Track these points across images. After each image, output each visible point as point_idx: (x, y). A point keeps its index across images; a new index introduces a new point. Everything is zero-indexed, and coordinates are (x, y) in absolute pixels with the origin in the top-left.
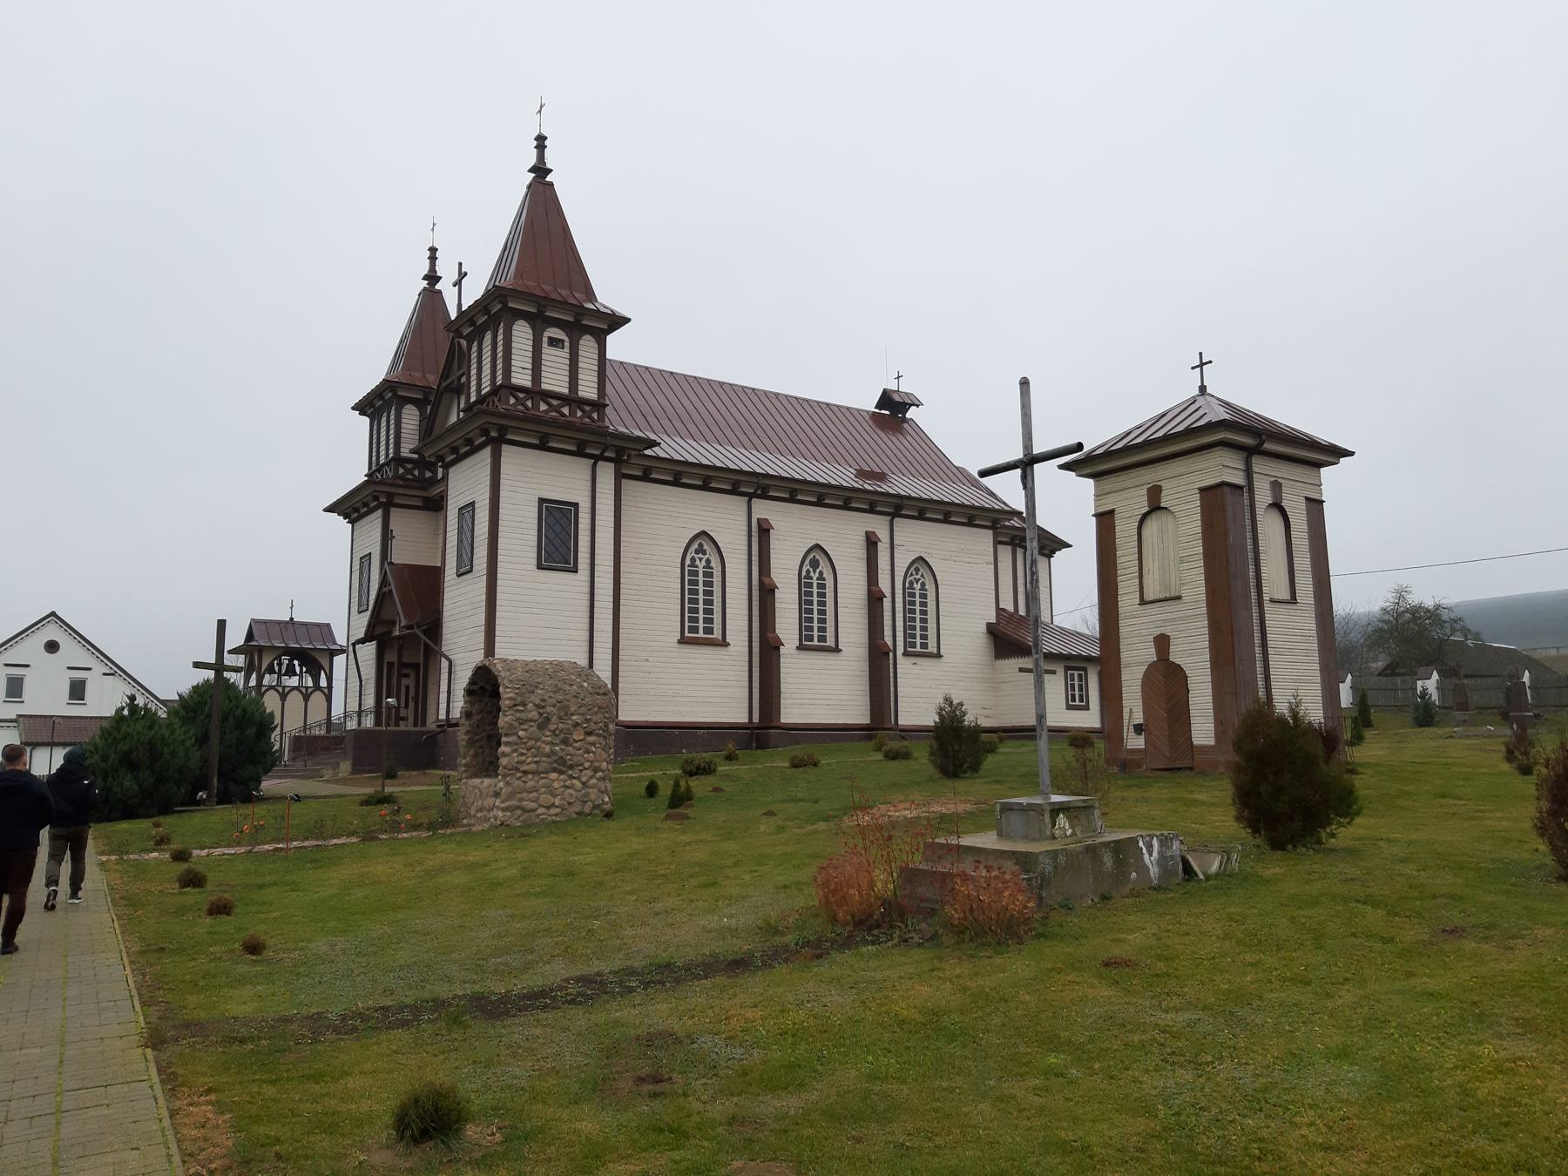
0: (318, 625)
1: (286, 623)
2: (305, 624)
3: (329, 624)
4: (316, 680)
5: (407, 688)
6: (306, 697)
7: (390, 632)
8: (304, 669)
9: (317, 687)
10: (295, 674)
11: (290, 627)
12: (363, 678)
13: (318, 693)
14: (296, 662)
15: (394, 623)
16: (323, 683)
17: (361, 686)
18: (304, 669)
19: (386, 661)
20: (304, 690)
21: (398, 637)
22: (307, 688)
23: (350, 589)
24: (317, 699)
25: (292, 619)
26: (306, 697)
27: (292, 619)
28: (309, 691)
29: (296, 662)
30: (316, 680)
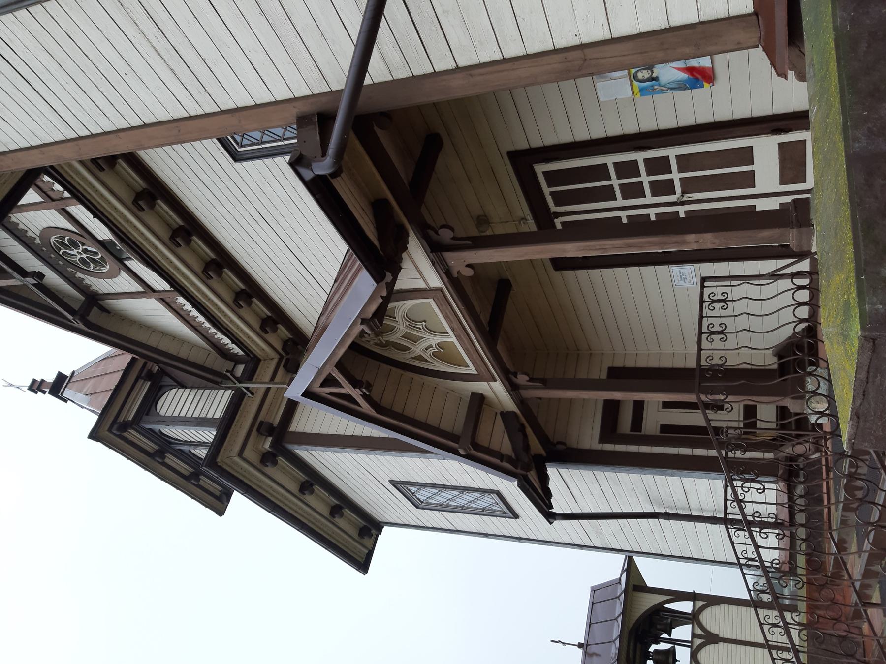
0: (593, 604)
1: (586, 652)
2: (590, 624)
3: (592, 588)
4: (680, 618)
5: (667, 405)
6: (712, 639)
7: (506, 416)
8: (665, 636)
9: (693, 618)
10: (672, 652)
11: (592, 649)
12: (648, 509)
13: (705, 617)
14: (653, 648)
15: (479, 400)
16: (685, 607)
17: (667, 516)
18: (665, 636)
19: (599, 447)
20: (698, 642)
21: (513, 388)
22: (694, 635)
23: (486, 535)
24: (712, 618)
25: (580, 646)
26: (712, 639)
27: (580, 646)
28: (699, 631)
29: (653, 648)
30: (680, 618)
